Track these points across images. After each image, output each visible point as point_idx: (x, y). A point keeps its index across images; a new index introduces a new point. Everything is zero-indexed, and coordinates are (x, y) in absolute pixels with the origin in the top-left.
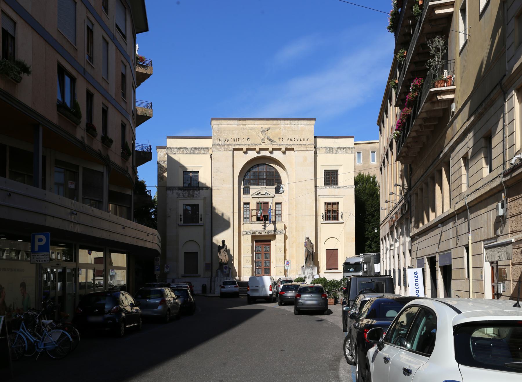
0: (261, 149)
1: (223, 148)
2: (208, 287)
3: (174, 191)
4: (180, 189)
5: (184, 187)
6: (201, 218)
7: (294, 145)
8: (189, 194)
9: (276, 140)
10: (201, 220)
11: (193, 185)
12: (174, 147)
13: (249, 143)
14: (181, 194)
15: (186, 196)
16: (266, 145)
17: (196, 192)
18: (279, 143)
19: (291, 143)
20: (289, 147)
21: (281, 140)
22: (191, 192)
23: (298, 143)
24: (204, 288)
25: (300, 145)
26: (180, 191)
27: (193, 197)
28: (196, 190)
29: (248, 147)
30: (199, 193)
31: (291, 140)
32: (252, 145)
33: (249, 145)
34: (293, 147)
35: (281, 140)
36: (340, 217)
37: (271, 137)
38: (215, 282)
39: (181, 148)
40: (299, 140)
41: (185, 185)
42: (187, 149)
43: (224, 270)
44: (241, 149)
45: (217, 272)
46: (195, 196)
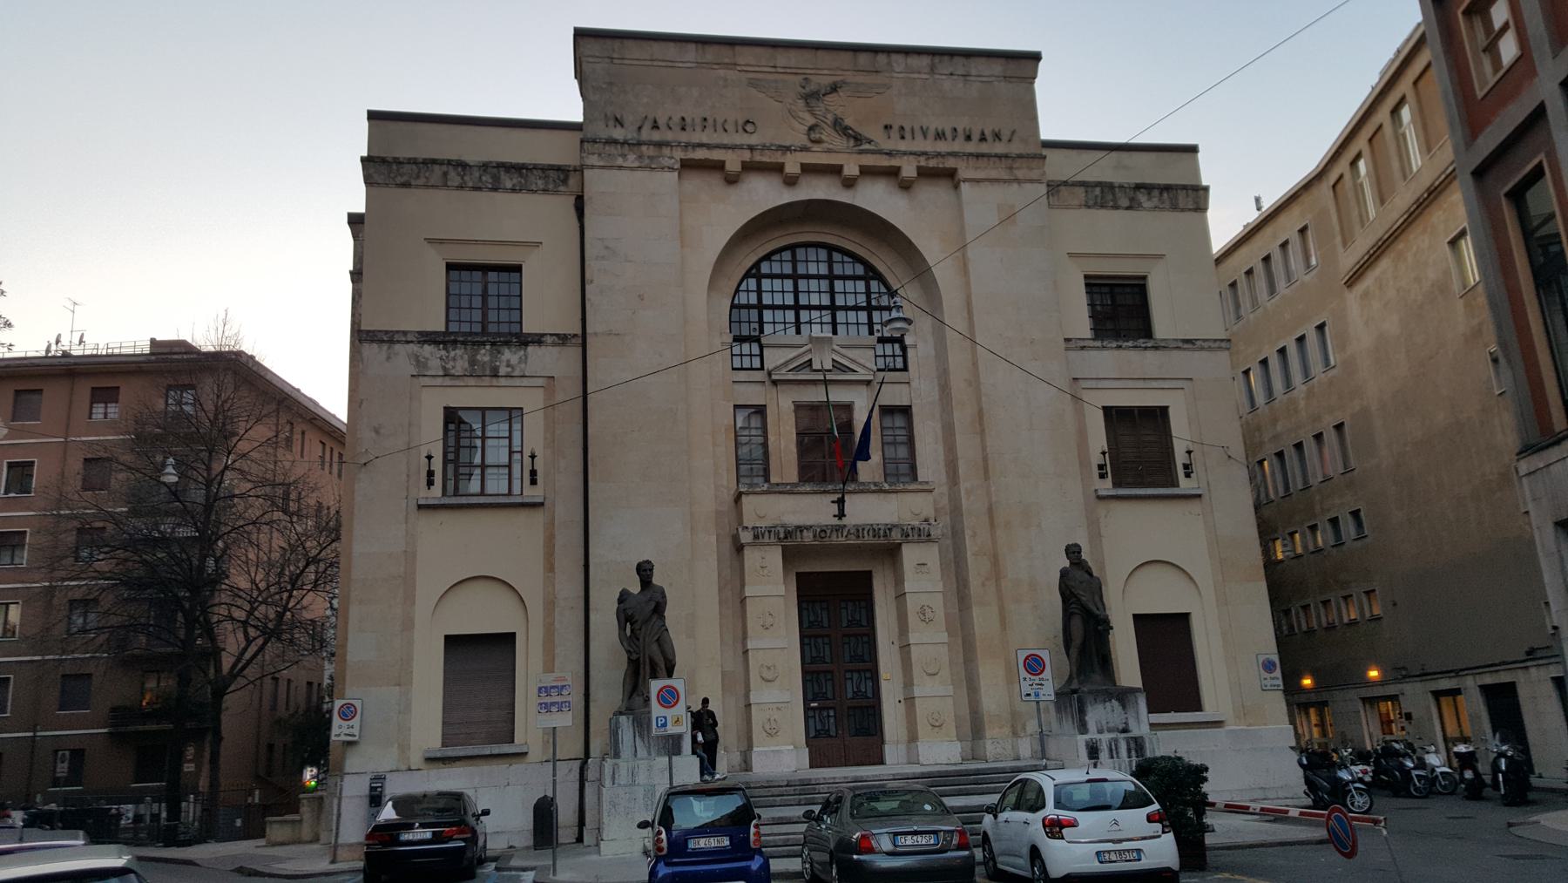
0: (808, 169)
1: (632, 157)
2: (566, 813)
3: (397, 347)
4: (428, 338)
5: (447, 333)
6: (533, 473)
7: (954, 154)
8: (473, 362)
9: (874, 132)
10: (533, 482)
11: (492, 328)
12: (403, 153)
13: (753, 140)
14: (435, 366)
15: (458, 371)
16: (829, 151)
17: (508, 355)
18: (888, 145)
19: (942, 147)
20: (932, 163)
21: (895, 133)
22: (484, 355)
23: (971, 147)
24: (544, 813)
25: (978, 156)
26: (428, 349)
27: (495, 375)
28: (507, 343)
29: (747, 156)
30: (524, 360)
31: (940, 136)
32: (765, 148)
33: (751, 148)
34: (950, 163)
35: (895, 133)
36: (1181, 472)
37: (848, 122)
38: (600, 782)
39: (434, 162)
40: (976, 137)
41: (454, 327)
42: (462, 166)
43: (656, 710)
44: (719, 166)
45: (614, 733)
46: (503, 371)
